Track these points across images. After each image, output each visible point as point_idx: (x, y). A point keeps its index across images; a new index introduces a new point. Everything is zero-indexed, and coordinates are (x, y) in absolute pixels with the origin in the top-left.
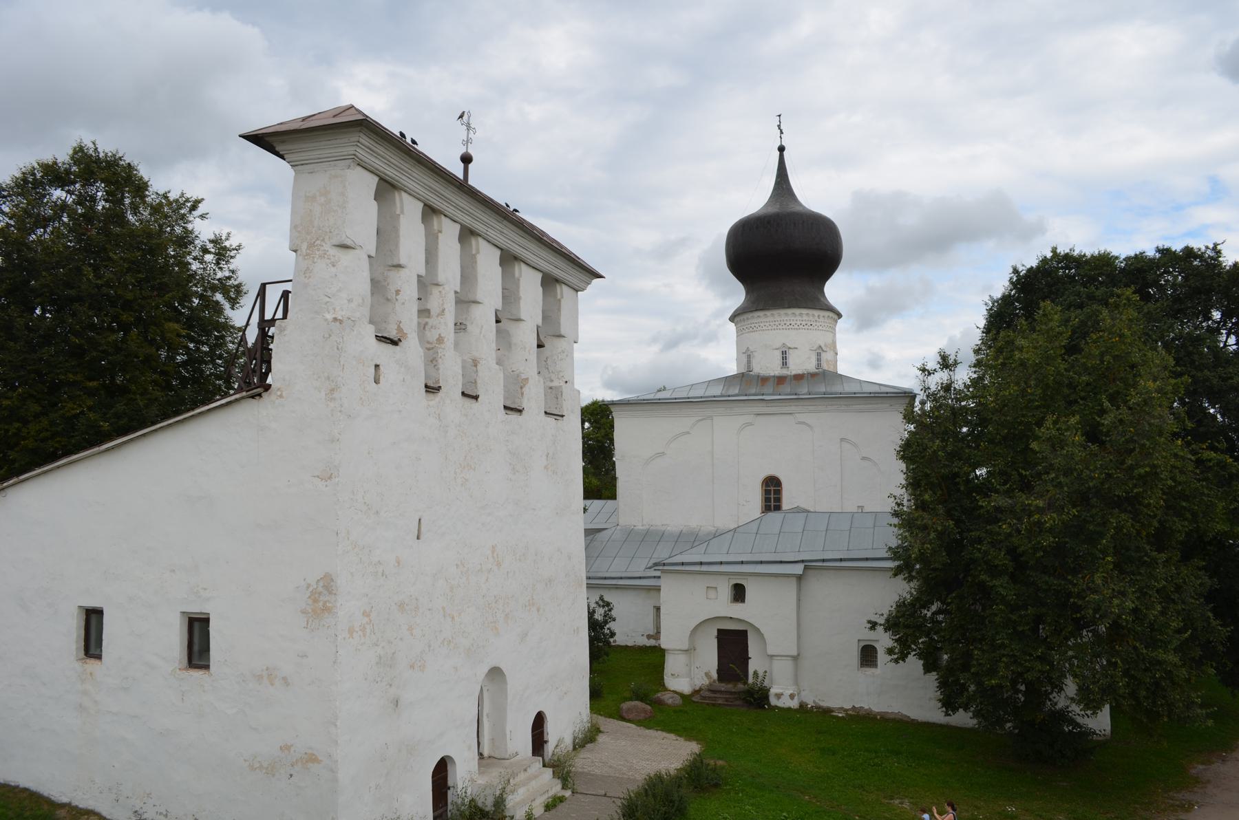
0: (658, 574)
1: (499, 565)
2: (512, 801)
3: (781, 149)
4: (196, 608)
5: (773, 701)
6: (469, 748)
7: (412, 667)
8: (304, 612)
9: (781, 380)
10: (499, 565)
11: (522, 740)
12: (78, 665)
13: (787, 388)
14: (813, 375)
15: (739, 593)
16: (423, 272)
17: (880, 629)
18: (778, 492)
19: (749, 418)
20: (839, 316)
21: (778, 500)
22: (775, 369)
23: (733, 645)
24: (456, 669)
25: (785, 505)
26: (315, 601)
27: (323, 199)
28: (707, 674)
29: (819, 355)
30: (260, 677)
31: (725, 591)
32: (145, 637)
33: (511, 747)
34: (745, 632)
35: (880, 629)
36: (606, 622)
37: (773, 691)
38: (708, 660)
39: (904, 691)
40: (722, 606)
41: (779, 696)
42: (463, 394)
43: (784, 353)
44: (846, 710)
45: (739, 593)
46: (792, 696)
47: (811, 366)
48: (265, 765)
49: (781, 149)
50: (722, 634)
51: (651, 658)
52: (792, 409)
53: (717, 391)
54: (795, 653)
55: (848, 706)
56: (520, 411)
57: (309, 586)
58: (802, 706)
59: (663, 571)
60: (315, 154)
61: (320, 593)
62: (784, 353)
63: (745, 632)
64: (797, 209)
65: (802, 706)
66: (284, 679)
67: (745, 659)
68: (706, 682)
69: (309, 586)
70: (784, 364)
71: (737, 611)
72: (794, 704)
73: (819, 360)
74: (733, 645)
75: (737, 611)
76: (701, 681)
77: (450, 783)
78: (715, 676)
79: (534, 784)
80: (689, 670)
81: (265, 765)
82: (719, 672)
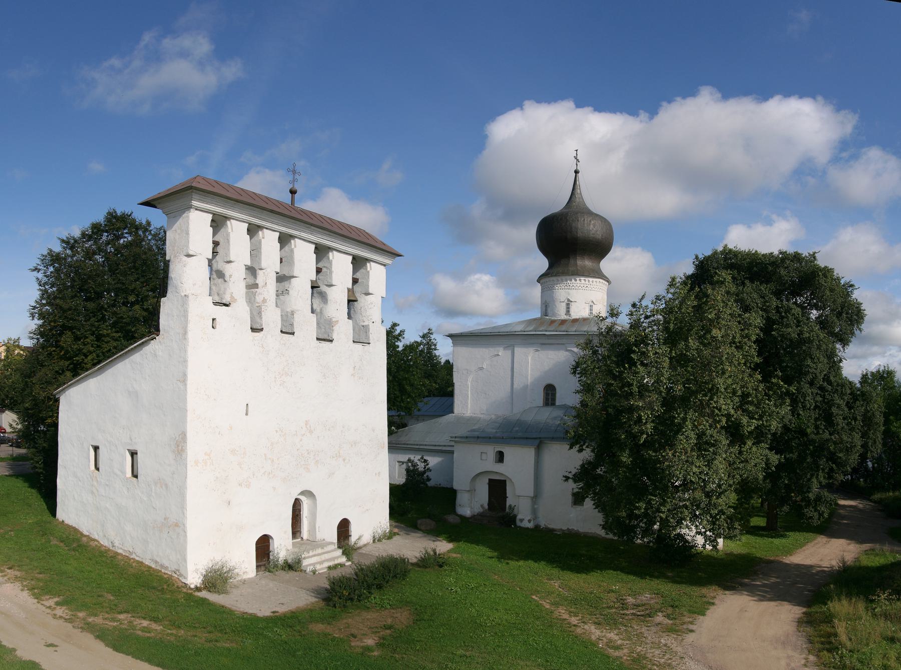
0: (453, 443)
1: (311, 432)
2: (305, 563)
5: (518, 523)
6: (285, 532)
7: (240, 485)
9: (563, 322)
10: (311, 432)
11: (332, 535)
13: (564, 328)
14: (585, 320)
15: (500, 457)
16: (249, 263)
17: (570, 481)
18: (554, 395)
21: (554, 399)
22: (563, 316)
24: (274, 488)
25: (557, 403)
28: (482, 506)
29: (591, 306)
33: (319, 536)
34: (505, 481)
35: (570, 481)
36: (424, 472)
37: (519, 517)
39: (587, 519)
40: (489, 464)
41: (521, 520)
42: (281, 331)
43: (568, 305)
46: (529, 521)
50: (491, 482)
51: (449, 495)
52: (564, 341)
55: (564, 528)
56: (331, 341)
58: (537, 527)
59: (456, 442)
62: (568, 305)
63: (505, 481)
65: (537, 527)
67: (505, 497)
68: (481, 510)
70: (568, 312)
72: (530, 525)
73: (591, 310)
74: (498, 488)
76: (477, 510)
77: (271, 549)
78: (486, 507)
79: (327, 556)
80: (472, 502)
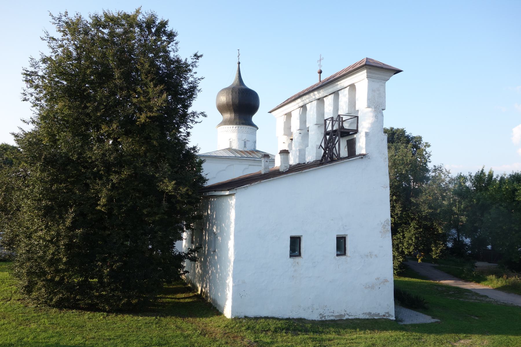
3: (239, 63)
8: (381, 232)
12: (292, 260)
26: (384, 228)
27: (378, 92)
30: (367, 256)
32: (318, 246)
43: (245, 142)
47: (252, 148)
48: (370, 286)
49: (239, 63)
57: (382, 223)
60: (377, 76)
66: (376, 255)
69: (382, 223)
81: (370, 286)
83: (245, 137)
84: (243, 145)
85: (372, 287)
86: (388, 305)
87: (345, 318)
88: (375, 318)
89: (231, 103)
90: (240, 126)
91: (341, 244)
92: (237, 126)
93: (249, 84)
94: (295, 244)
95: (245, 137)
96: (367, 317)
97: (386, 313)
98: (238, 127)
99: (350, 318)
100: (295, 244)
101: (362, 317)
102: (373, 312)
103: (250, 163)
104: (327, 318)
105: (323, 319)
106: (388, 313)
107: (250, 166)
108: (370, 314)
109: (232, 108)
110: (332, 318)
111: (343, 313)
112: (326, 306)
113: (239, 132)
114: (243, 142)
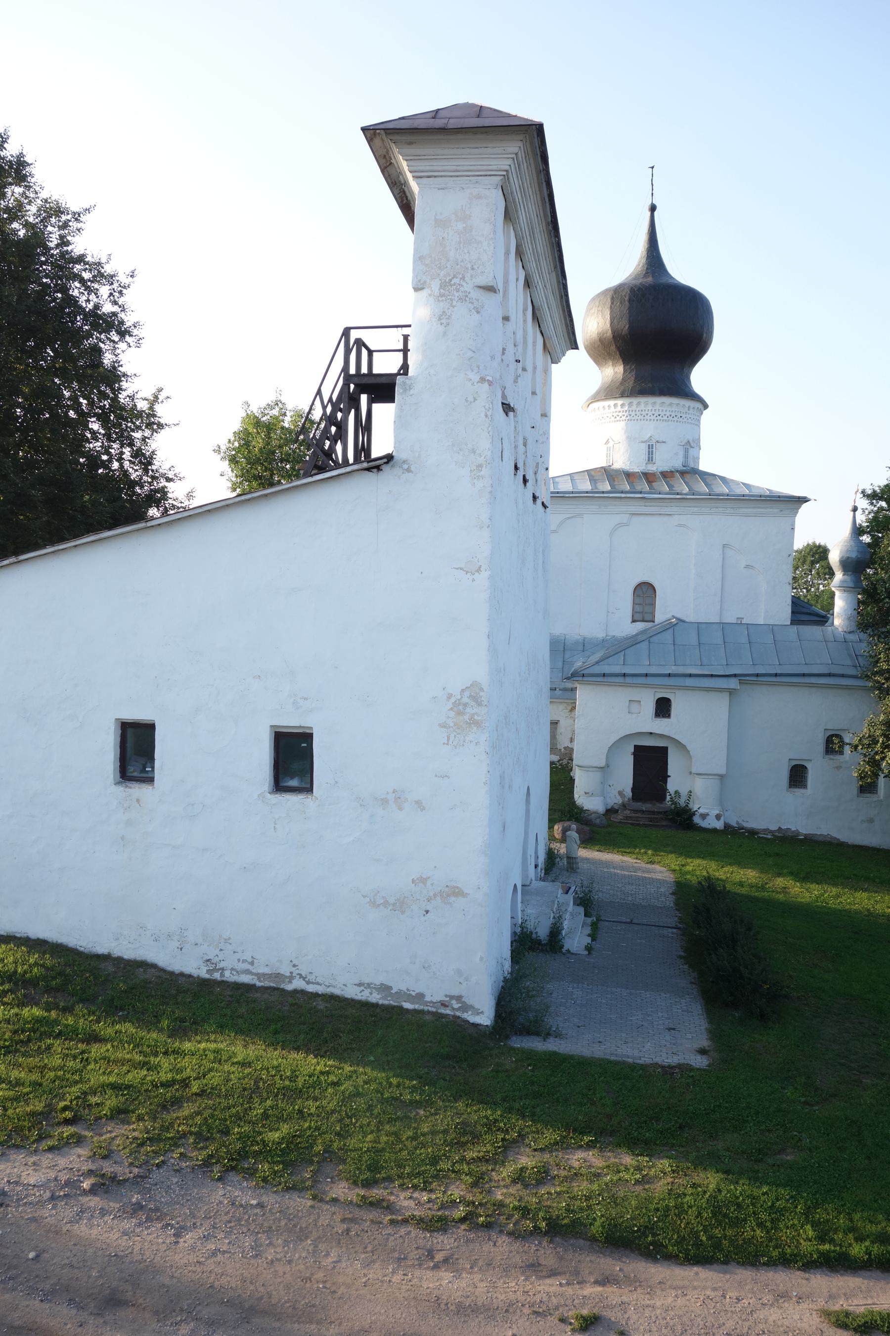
3: (653, 208)
4: (291, 721)
5: (697, 819)
8: (443, 726)
12: (120, 791)
15: (663, 708)
19: (624, 518)
20: (706, 406)
23: (651, 762)
26: (459, 713)
27: (460, 226)
28: (620, 793)
29: (686, 451)
30: (384, 802)
31: (649, 706)
38: (624, 777)
40: (644, 721)
41: (704, 816)
43: (650, 447)
44: (772, 832)
45: (663, 708)
46: (718, 817)
47: (677, 463)
48: (392, 900)
49: (653, 208)
53: (586, 485)
54: (723, 771)
55: (774, 827)
57: (450, 696)
58: (727, 826)
60: (451, 165)
61: (466, 705)
63: (664, 751)
64: (664, 280)
65: (727, 826)
66: (418, 803)
67: (665, 777)
68: (619, 800)
69: (450, 696)
71: (661, 726)
72: (719, 825)
73: (686, 457)
74: (651, 762)
75: (661, 726)
76: (614, 800)
78: (629, 793)
81: (392, 900)
82: (633, 790)
83: (651, 430)
84: (644, 456)
85: (400, 905)
86: (459, 972)
87: (290, 987)
88: (407, 1006)
89: (609, 334)
90: (635, 400)
91: (292, 758)
92: (626, 401)
93: (681, 269)
94: (136, 749)
95: (651, 430)
96: (375, 998)
97: (452, 997)
98: (630, 404)
99: (311, 988)
100: (136, 749)
101: (352, 993)
102: (398, 985)
103: (633, 509)
104: (229, 977)
105: (217, 976)
106: (459, 998)
107: (635, 518)
108: (384, 988)
109: (613, 348)
110: (245, 979)
111: (285, 970)
112: (227, 940)
113: (631, 418)
114: (644, 447)
